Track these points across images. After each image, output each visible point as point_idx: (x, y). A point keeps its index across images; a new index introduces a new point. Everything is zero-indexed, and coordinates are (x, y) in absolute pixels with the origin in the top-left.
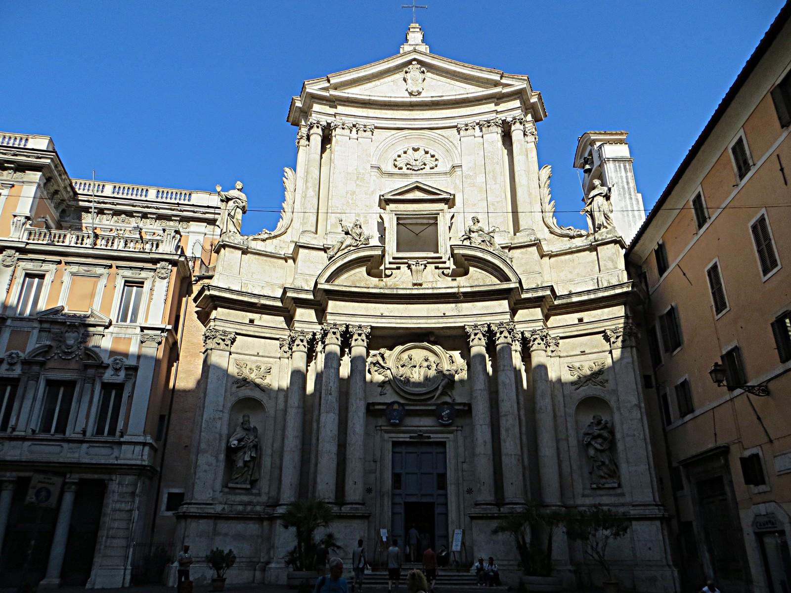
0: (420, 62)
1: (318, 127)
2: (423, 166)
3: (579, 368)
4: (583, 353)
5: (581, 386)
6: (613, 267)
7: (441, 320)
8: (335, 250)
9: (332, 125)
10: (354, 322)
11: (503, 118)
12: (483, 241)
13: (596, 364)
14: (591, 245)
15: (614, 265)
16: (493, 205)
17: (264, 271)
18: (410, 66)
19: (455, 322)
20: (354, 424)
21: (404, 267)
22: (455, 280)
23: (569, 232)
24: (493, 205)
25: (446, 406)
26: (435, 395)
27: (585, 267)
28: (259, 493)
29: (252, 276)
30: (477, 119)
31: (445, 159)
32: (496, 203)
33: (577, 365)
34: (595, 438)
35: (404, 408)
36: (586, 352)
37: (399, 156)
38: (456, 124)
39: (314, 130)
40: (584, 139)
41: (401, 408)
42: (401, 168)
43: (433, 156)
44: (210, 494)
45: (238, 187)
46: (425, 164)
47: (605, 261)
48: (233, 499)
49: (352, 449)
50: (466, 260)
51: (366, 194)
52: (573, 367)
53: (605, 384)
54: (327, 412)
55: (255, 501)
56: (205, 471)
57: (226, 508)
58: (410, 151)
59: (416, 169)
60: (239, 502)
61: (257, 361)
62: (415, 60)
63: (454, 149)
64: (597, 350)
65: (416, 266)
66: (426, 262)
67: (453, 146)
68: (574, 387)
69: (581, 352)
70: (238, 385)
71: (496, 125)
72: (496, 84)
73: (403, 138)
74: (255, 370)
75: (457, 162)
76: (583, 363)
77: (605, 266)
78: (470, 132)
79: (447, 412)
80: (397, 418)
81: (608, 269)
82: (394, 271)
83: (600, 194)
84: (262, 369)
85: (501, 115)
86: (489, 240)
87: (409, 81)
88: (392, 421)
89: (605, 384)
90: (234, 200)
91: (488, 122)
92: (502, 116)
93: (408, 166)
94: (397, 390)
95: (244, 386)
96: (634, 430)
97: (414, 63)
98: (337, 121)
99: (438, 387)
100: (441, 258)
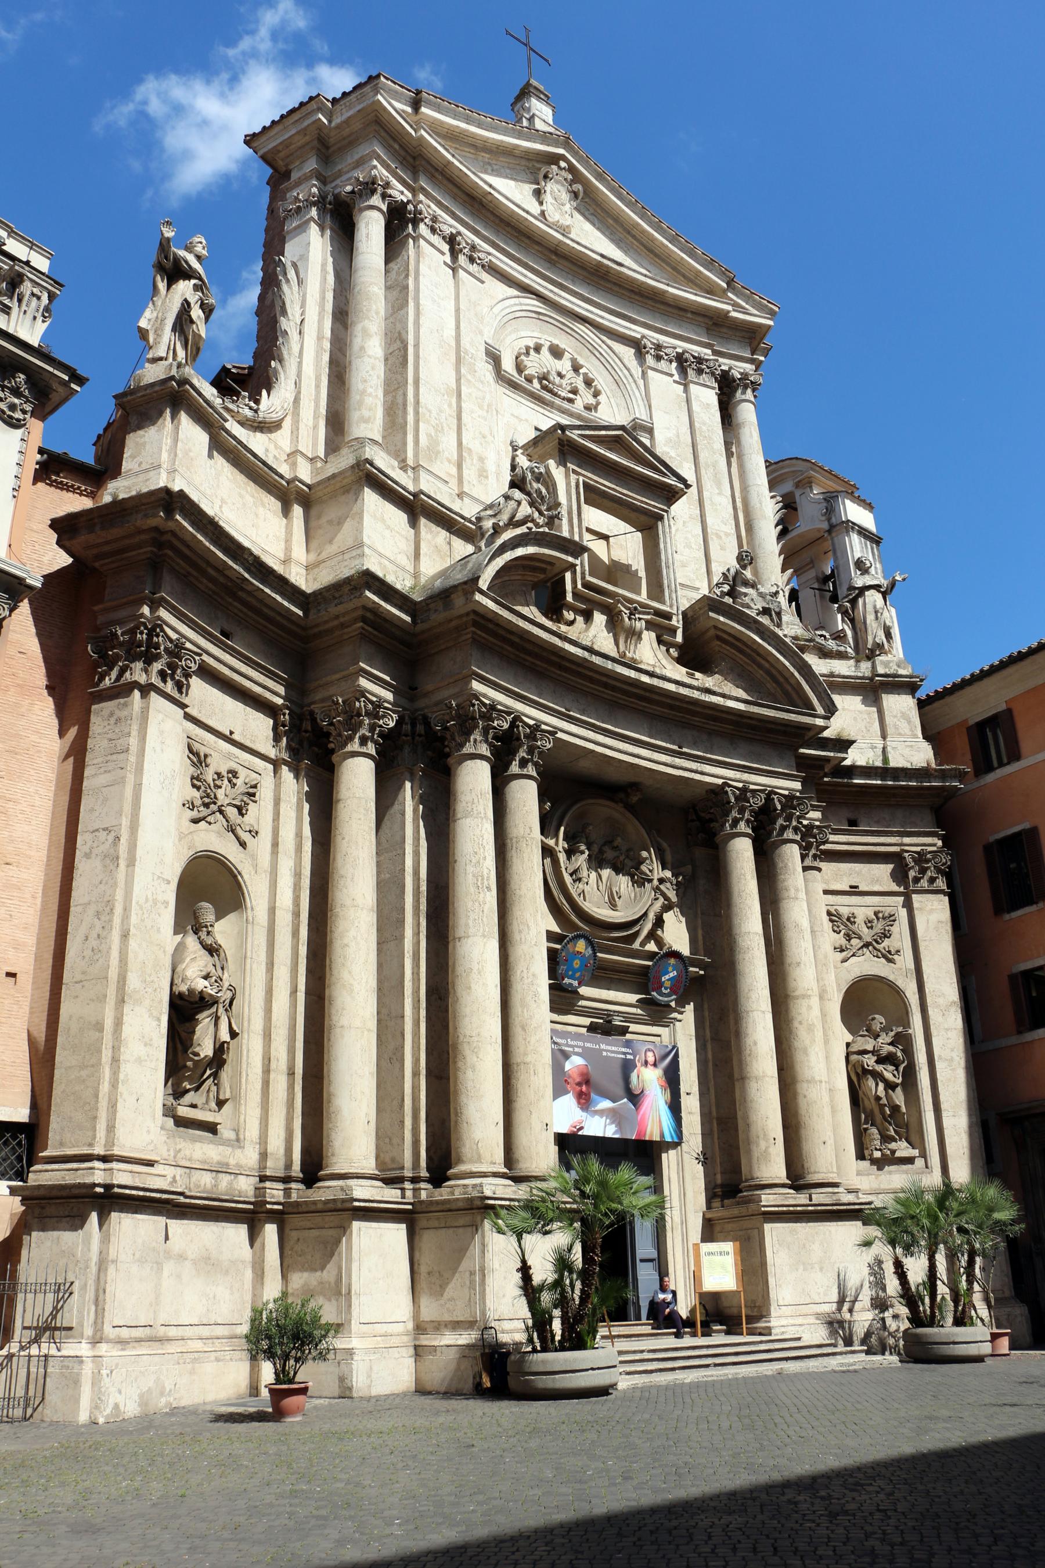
0: (572, 169)
1: (384, 196)
2: (571, 396)
3: (848, 919)
4: (854, 891)
5: (853, 955)
6: (908, 732)
7: (678, 761)
8: (504, 518)
9: (410, 207)
10: (532, 714)
11: (723, 368)
12: (766, 611)
13: (880, 915)
14: (871, 679)
15: (911, 730)
16: (719, 537)
17: (244, 504)
18: (554, 167)
19: (702, 773)
20: (534, 975)
21: (599, 619)
22: (693, 675)
23: (823, 642)
24: (719, 537)
25: (672, 961)
26: (636, 934)
27: (855, 719)
28: (238, 1140)
29: (221, 507)
30: (681, 346)
31: (612, 400)
32: (723, 537)
33: (845, 911)
34: (880, 1061)
35: (595, 953)
36: (861, 889)
37: (528, 348)
38: (639, 336)
39: (376, 200)
40: (782, 468)
41: (590, 951)
42: (529, 380)
43: (588, 383)
44: (148, 1132)
45: (199, 249)
46: (575, 391)
47: (895, 717)
48: (188, 1153)
49: (533, 1040)
50: (718, 638)
51: (481, 407)
52: (839, 916)
53: (896, 957)
54: (484, 936)
55: (232, 1162)
56: (139, 1061)
57: (178, 1178)
58: (545, 351)
59: (563, 394)
60: (204, 1162)
61: (229, 756)
62: (563, 157)
63: (633, 384)
64: (881, 889)
65: (630, 619)
66: (649, 617)
67: (631, 380)
68: (840, 956)
69: (851, 887)
70: (195, 814)
71: (713, 374)
72: (710, 290)
73: (534, 315)
74: (226, 782)
75: (642, 414)
76: (856, 910)
77: (896, 727)
78: (663, 365)
79: (671, 975)
80: (578, 975)
81: (900, 734)
82: (580, 619)
83: (876, 587)
84: (239, 782)
85: (721, 360)
86: (777, 610)
87: (548, 198)
88: (566, 981)
89: (896, 957)
90: (193, 281)
91: (700, 360)
92: (725, 363)
93: (545, 382)
94: (566, 907)
95: (204, 819)
96: (952, 1050)
97: (563, 164)
98: (428, 207)
99: (645, 914)
100: (668, 616)
